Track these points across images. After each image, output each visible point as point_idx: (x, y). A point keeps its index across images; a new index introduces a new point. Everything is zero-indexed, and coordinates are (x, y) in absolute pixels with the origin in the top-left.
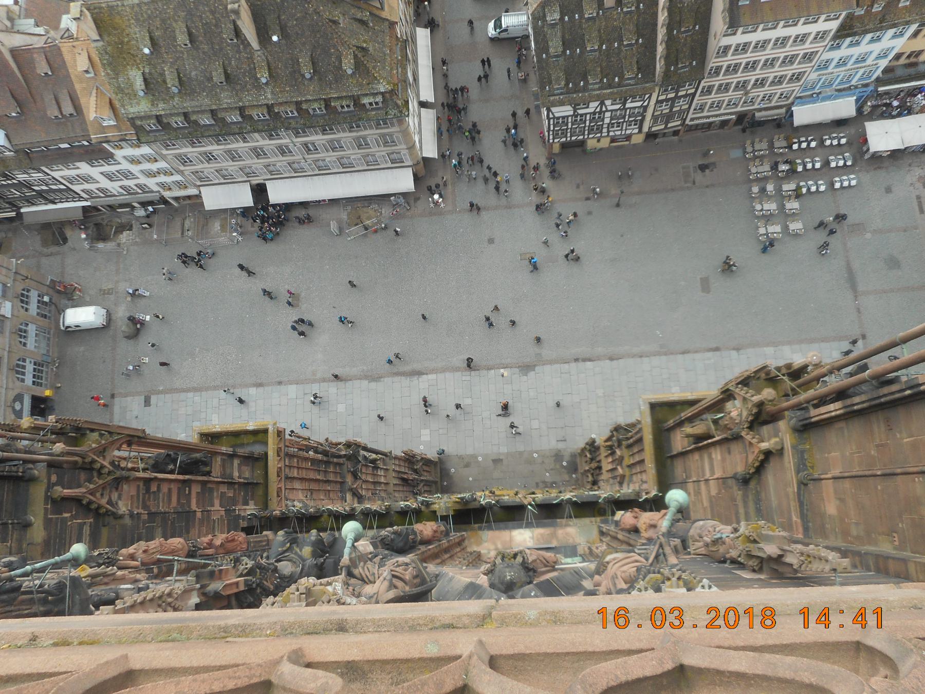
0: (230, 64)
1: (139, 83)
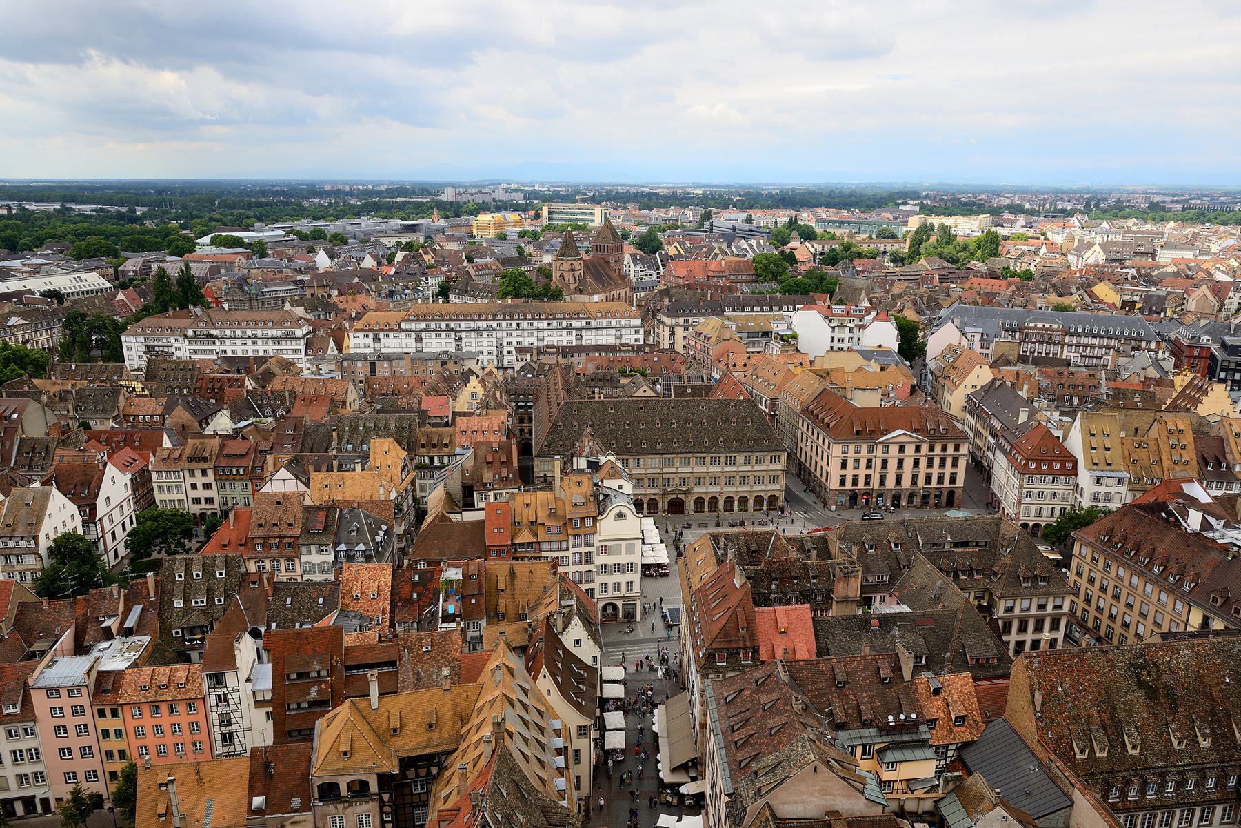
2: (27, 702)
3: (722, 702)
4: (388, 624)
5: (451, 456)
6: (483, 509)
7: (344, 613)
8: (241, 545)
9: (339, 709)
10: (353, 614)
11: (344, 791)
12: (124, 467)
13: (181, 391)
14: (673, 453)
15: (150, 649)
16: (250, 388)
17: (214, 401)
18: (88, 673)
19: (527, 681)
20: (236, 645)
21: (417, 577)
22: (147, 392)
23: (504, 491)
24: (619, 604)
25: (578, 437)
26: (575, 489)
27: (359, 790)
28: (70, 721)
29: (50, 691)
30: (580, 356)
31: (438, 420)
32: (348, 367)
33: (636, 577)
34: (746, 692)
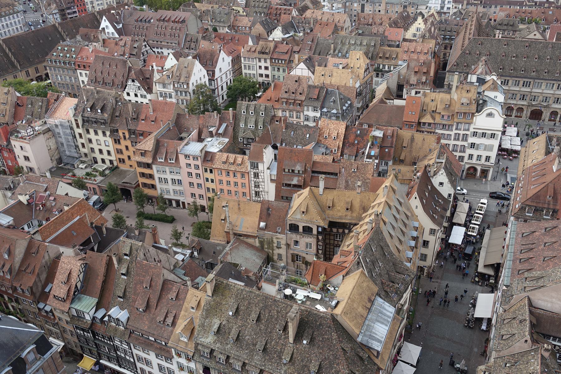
0: (271, 343)
1: (216, 327)
2: (177, 159)
3: (520, 236)
4: (340, 154)
5: (395, 66)
6: (405, 99)
7: (318, 143)
8: (276, 101)
9: (304, 190)
10: (323, 146)
11: (301, 229)
12: (229, 53)
13: (261, 14)
14: (542, 79)
15: (228, 145)
16: (295, 15)
17: (276, 21)
18: (201, 151)
19: (403, 198)
20: (264, 150)
21: (359, 132)
22: (245, 14)
23: (422, 91)
24: (479, 168)
25: (476, 62)
26: (465, 94)
27: (308, 230)
28: (194, 171)
29: (187, 156)
30: (496, 7)
31: (393, 43)
32: (349, 6)
33: (493, 154)
34: (537, 233)
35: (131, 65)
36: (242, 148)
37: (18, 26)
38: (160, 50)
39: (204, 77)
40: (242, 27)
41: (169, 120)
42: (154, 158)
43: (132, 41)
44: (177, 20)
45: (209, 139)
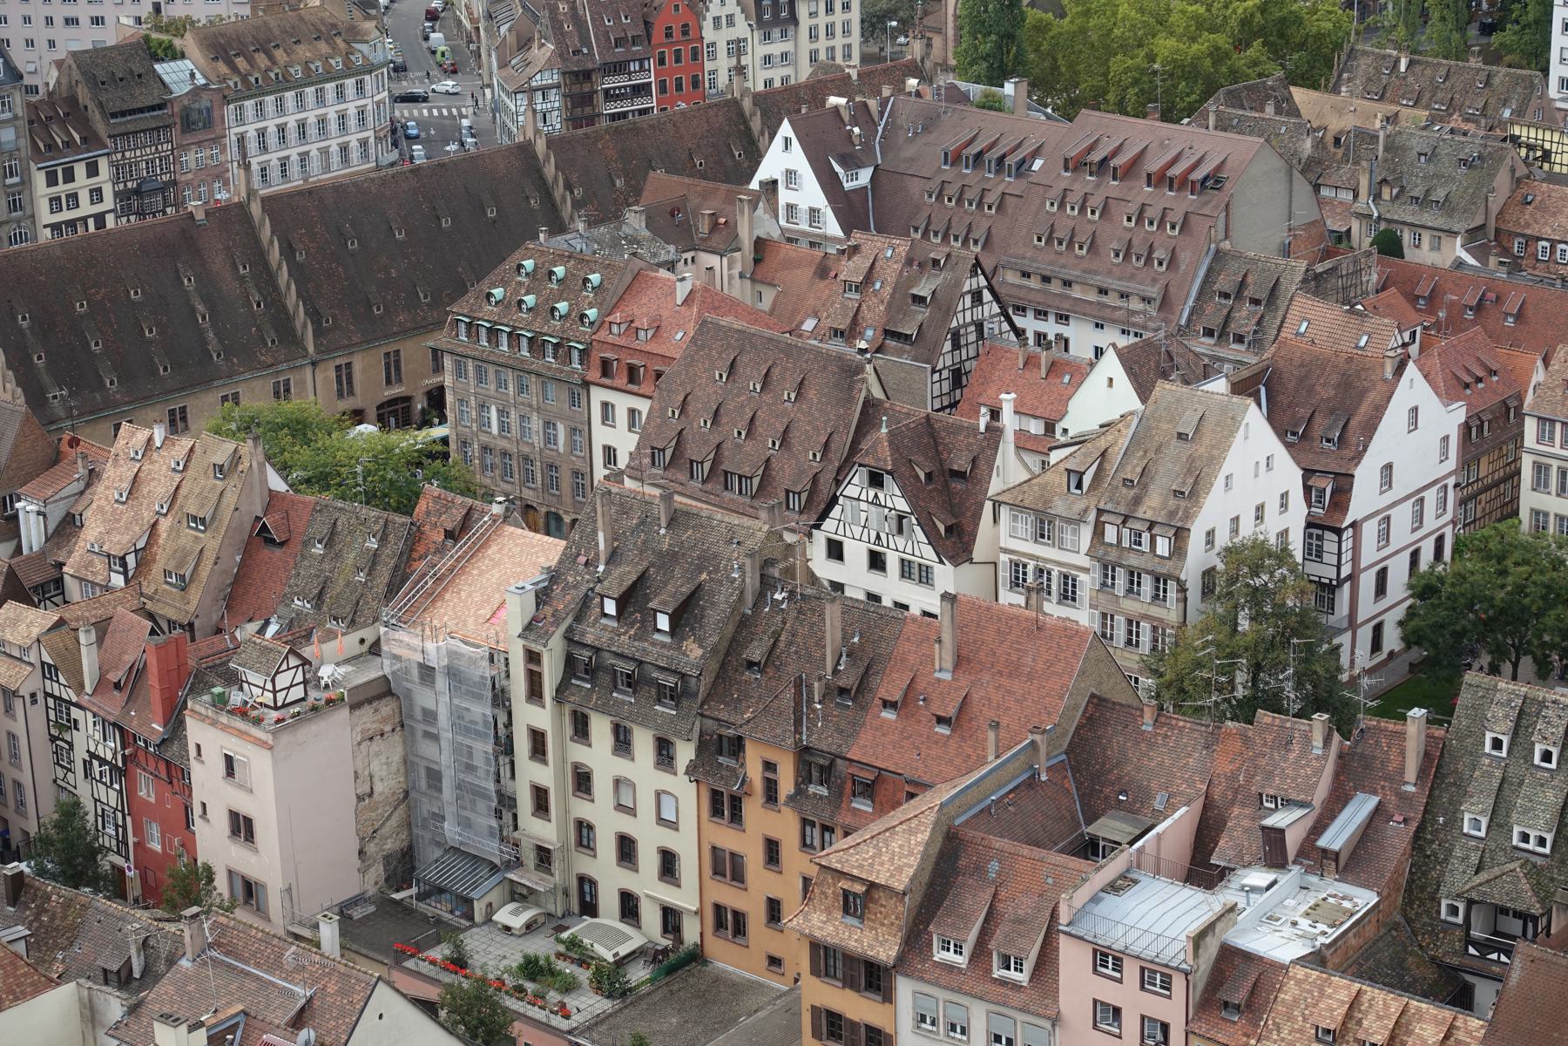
2: (1046, 963)
12: (1452, 387)
15: (1370, 931)
18: (1199, 939)
29: (1106, 959)
35: (877, 393)
36: (1455, 961)
37: (353, 140)
38: (1051, 328)
39: (1284, 505)
40: (1553, 243)
41: (1036, 729)
42: (915, 940)
43: (909, 262)
44: (1176, 171)
45: (1258, 877)
